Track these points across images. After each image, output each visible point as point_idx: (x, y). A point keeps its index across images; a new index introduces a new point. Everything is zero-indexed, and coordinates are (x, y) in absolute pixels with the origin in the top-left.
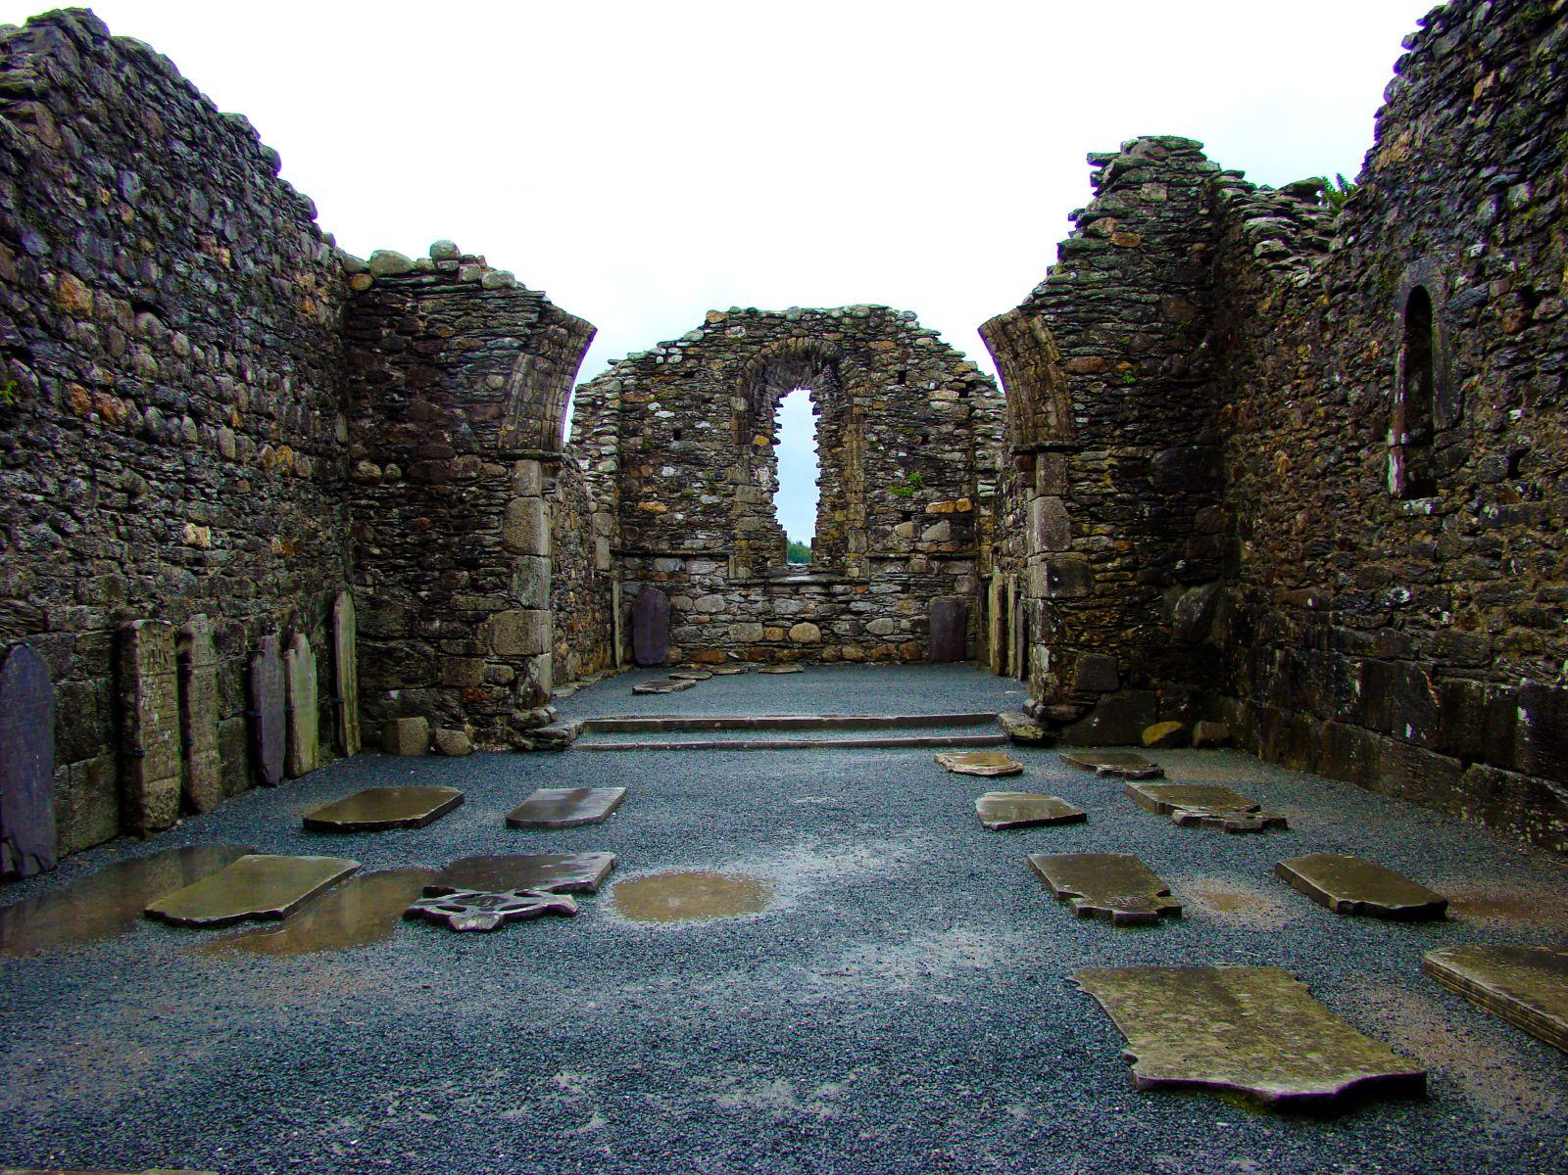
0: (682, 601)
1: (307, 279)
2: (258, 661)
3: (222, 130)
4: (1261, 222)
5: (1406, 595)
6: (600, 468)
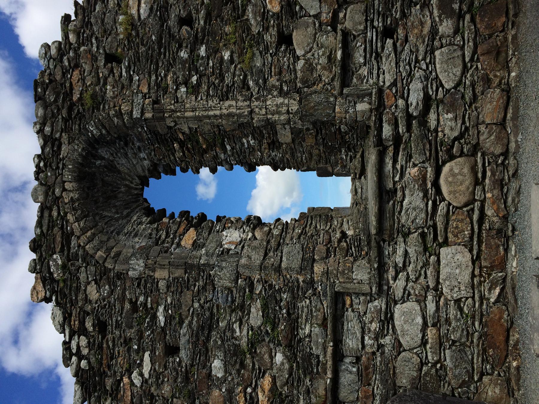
0: (406, 373)
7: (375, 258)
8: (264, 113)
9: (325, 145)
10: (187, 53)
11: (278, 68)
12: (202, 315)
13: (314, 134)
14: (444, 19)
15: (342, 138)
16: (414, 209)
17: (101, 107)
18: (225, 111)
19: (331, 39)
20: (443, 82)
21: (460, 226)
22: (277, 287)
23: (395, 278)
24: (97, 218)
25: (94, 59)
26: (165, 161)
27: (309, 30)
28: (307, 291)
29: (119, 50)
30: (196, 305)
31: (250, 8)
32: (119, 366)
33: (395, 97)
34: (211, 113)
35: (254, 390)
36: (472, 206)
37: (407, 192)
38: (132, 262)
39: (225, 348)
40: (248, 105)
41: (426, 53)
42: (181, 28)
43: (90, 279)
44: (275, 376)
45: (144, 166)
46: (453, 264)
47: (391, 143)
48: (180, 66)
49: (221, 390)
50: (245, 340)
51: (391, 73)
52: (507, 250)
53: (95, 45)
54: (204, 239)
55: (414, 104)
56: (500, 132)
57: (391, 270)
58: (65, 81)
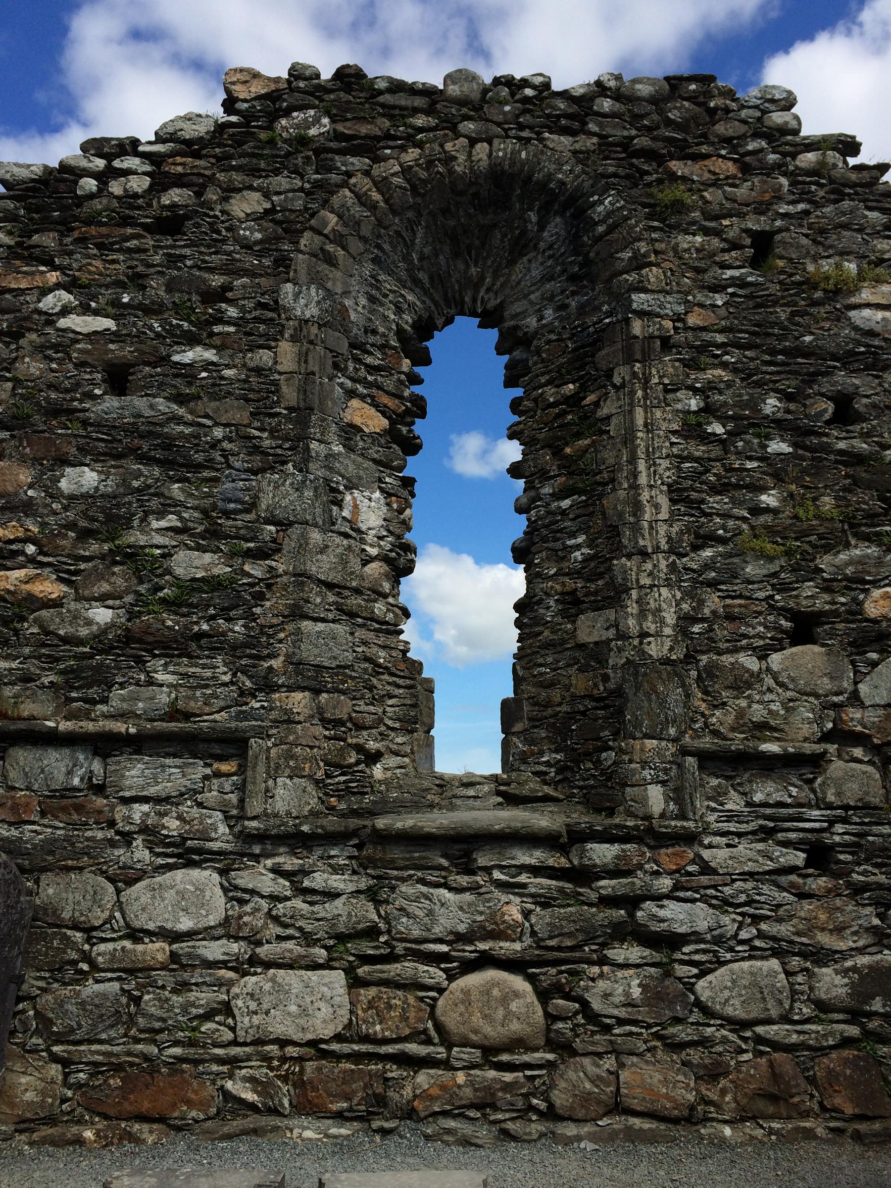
0: (68, 894)
7: (322, 827)
8: (642, 582)
9: (570, 717)
10: (773, 413)
11: (741, 613)
12: (196, 445)
13: (595, 692)
14: (850, 978)
15: (588, 755)
16: (430, 913)
17: (656, 224)
18: (645, 496)
19: (806, 730)
20: (709, 977)
21: (392, 1014)
22: (257, 610)
23: (277, 871)
24: (410, 214)
25: (762, 208)
26: (535, 364)
27: (826, 680)
28: (250, 677)
29: (781, 263)
30: (218, 433)
31: (873, 550)
32: (84, 262)
33: (677, 871)
34: (642, 466)
35: (32, 561)
36: (436, 1040)
37: (468, 897)
38: (313, 291)
39: (125, 495)
40: (658, 548)
41: (774, 939)
42: (829, 399)
43: (275, 198)
44: (61, 605)
45: (525, 318)
46: (308, 999)
47: (576, 862)
48: (745, 398)
49: (31, 486)
50: (142, 540)
51: (730, 862)
52: (340, 1117)
53: (791, 208)
54: (364, 449)
55: (662, 913)
56: (599, 1102)
57: (296, 861)
58: (712, 144)
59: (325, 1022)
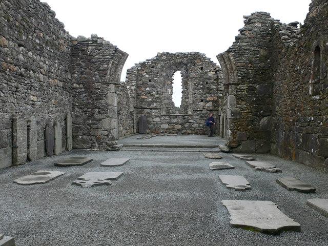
0: (150, 119)
1: (62, 41)
2: (48, 127)
3: (41, 6)
4: (283, 32)
5: (313, 118)
6: (132, 88)
59: (167, 128)
